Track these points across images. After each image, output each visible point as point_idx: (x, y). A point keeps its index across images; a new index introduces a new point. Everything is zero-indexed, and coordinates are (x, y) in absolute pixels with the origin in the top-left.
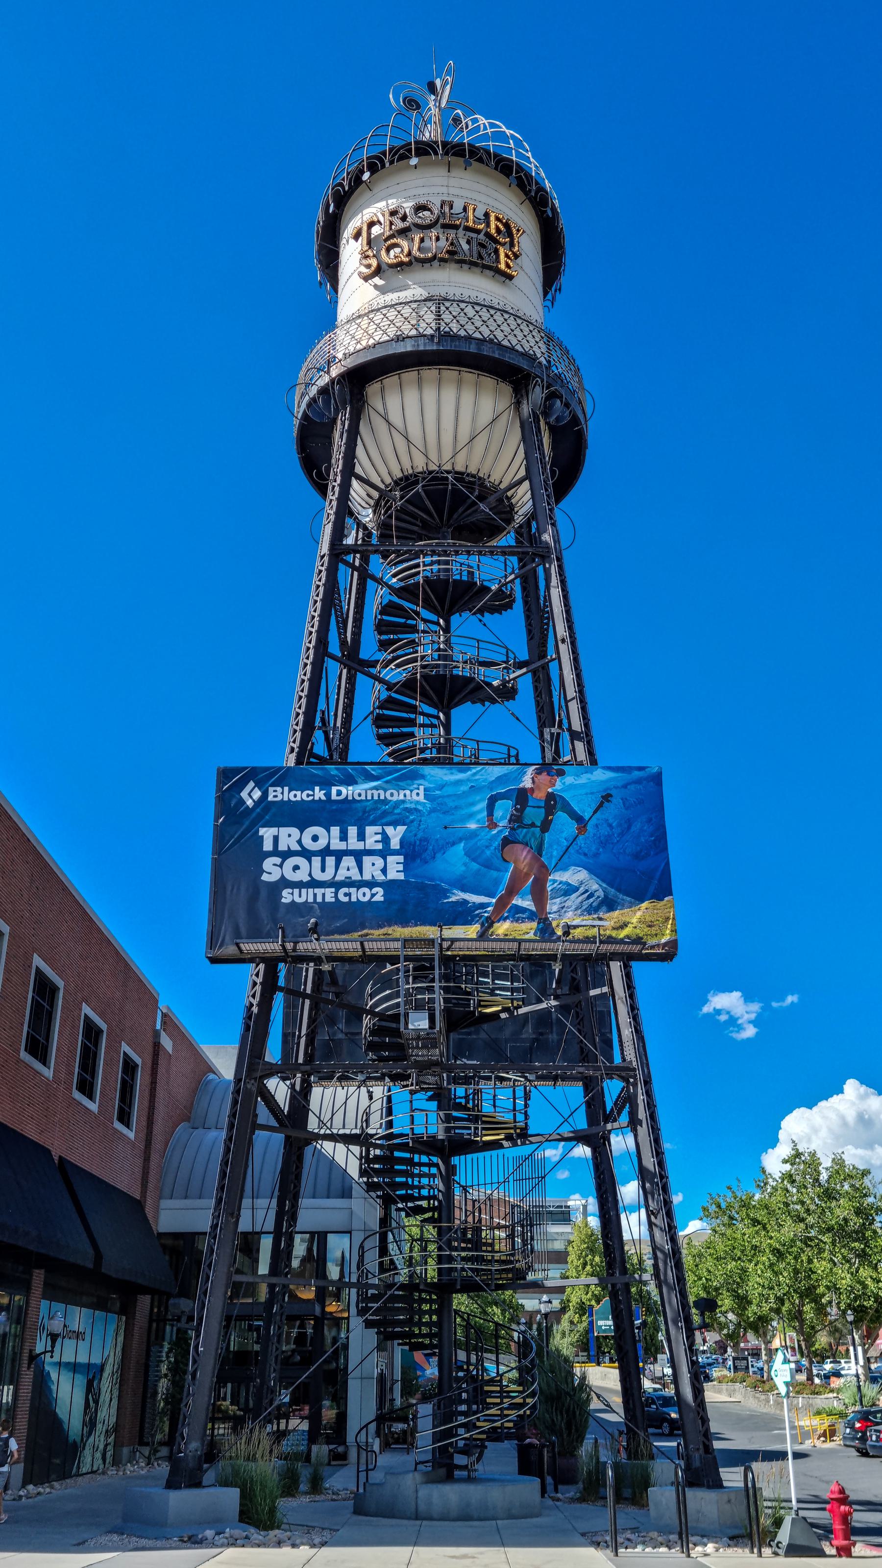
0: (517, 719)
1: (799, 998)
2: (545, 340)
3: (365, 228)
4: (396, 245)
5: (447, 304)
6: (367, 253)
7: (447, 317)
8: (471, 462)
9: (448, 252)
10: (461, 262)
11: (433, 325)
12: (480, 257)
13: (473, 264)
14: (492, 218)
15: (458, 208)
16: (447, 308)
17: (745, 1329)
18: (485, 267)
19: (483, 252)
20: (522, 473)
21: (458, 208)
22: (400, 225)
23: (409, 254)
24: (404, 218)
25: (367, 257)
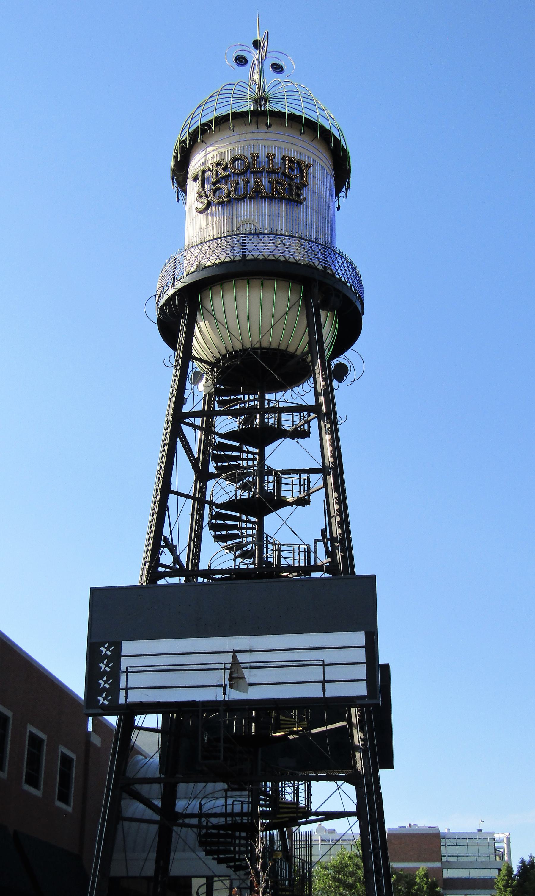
0: (295, 534)
1: (119, 720)
2: (322, 251)
3: (200, 173)
4: (219, 189)
5: (251, 237)
6: (201, 194)
7: (250, 247)
8: (272, 340)
9: (255, 192)
10: (265, 198)
11: (241, 253)
12: (278, 193)
13: (272, 198)
14: (287, 161)
15: (263, 157)
16: (250, 240)
17: (199, 826)
18: (282, 199)
19: (280, 189)
20: (307, 348)
21: (263, 157)
22: (223, 173)
23: (228, 196)
24: (225, 168)
25: (201, 196)
